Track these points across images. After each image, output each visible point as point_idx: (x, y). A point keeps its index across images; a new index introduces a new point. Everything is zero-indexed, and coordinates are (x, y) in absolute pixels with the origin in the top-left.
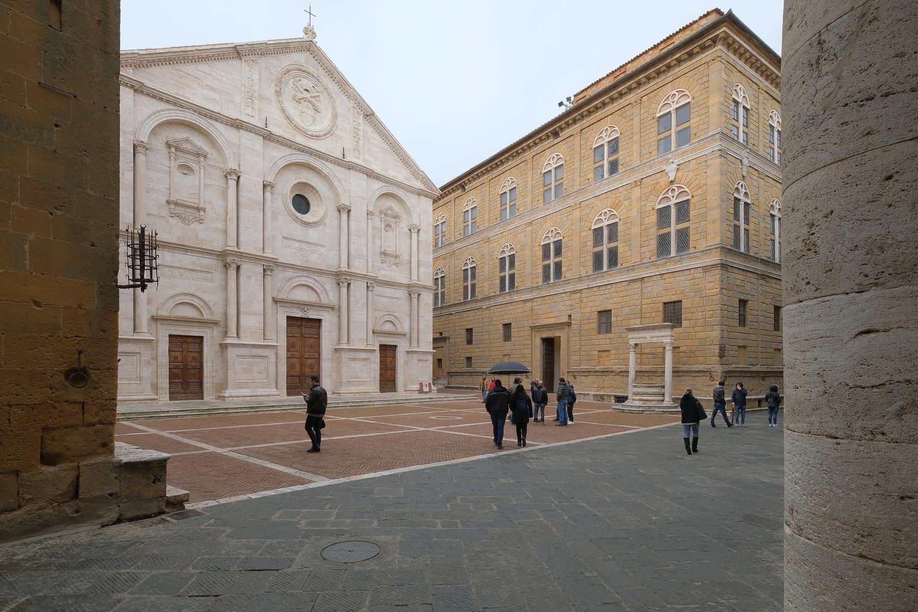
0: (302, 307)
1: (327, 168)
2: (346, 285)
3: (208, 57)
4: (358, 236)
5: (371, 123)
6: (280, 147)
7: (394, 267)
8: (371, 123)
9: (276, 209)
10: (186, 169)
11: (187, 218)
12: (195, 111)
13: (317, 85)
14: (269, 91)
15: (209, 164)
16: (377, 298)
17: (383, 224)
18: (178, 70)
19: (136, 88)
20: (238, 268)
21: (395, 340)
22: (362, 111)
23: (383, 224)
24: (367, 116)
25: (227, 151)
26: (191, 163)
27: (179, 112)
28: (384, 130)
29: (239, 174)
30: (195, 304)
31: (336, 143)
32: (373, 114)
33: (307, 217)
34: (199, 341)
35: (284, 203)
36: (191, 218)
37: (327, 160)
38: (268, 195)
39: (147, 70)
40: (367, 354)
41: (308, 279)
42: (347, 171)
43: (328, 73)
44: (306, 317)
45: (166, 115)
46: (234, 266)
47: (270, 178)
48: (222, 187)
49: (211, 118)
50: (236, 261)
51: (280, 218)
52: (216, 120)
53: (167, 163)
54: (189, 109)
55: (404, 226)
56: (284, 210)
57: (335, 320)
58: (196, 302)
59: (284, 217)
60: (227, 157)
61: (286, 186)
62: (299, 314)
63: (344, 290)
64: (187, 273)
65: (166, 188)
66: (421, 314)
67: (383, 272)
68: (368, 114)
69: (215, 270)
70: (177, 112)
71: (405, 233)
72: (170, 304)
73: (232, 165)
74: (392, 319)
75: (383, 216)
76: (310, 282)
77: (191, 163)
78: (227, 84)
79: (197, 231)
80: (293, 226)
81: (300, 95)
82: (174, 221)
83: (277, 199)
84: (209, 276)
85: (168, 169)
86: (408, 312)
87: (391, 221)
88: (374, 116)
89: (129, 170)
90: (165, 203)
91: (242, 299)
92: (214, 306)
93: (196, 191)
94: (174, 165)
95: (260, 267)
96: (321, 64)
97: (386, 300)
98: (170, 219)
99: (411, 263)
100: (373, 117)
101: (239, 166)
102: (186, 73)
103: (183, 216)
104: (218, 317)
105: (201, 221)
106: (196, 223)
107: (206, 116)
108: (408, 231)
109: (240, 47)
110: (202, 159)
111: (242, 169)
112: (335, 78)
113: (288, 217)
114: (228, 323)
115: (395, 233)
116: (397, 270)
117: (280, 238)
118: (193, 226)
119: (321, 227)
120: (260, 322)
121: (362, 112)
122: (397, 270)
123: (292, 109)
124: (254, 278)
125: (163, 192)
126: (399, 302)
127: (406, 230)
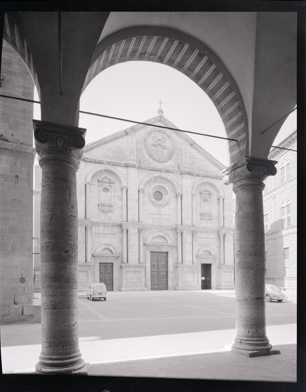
1: (170, 177)
7: (209, 221)
10: (106, 190)
17: (202, 199)
22: (188, 143)
23: (202, 199)
24: (192, 144)
29: (127, 188)
32: (195, 143)
33: (160, 202)
34: (112, 265)
35: (150, 197)
38: (141, 195)
47: (141, 187)
58: (110, 248)
61: (150, 189)
63: (179, 237)
64: (106, 235)
73: (124, 184)
74: (208, 249)
84: (116, 236)
86: (218, 245)
87: (207, 197)
94: (101, 189)
99: (219, 218)
101: (127, 184)
105: (111, 211)
108: (217, 201)
111: (129, 185)
118: (109, 214)
119: (167, 206)
126: (212, 240)
127: (216, 200)
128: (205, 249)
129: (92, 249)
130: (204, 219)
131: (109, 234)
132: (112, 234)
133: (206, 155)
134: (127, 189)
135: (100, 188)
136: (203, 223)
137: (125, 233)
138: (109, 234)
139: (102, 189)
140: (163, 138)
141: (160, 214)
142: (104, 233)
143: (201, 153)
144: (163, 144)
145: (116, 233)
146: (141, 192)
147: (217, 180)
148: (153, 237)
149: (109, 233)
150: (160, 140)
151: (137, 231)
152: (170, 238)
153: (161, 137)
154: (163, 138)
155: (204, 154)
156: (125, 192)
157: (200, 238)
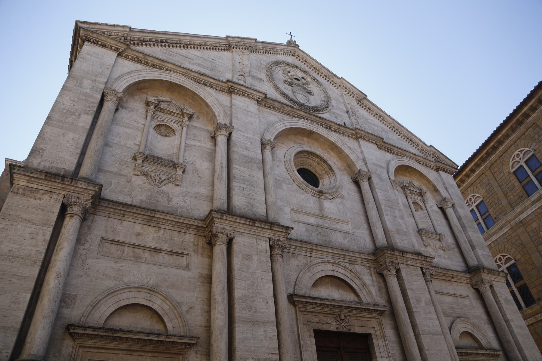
0: (338, 311)
2: (393, 271)
3: (200, 45)
6: (277, 114)
7: (441, 252)
8: (364, 107)
9: (279, 177)
11: (157, 178)
14: (263, 76)
15: (194, 126)
19: (121, 51)
20: (230, 243)
25: (217, 110)
26: (172, 124)
28: (379, 111)
30: (155, 307)
36: (164, 178)
38: (268, 154)
41: (336, 268)
43: (315, 70)
44: (345, 330)
45: (149, 75)
46: (223, 239)
48: (208, 149)
50: (226, 231)
51: (285, 186)
52: (205, 84)
53: (142, 121)
55: (432, 203)
56: (289, 177)
57: (390, 333)
58: (157, 304)
60: (216, 115)
62: (332, 326)
64: (147, 254)
65: (135, 144)
68: (361, 98)
69: (194, 251)
70: (161, 73)
71: (437, 212)
76: (340, 273)
79: (171, 196)
80: (303, 196)
82: (139, 181)
83: (278, 166)
84: (183, 261)
85: (142, 126)
87: (418, 199)
89: (88, 114)
90: (130, 160)
91: (238, 293)
92: (188, 312)
93: (175, 151)
95: (264, 242)
97: (449, 299)
98: (134, 178)
103: (153, 175)
104: (198, 329)
106: (170, 185)
109: (231, 39)
110: (186, 119)
113: (296, 186)
114: (213, 342)
115: (425, 211)
116: (446, 257)
117: (287, 210)
118: (164, 188)
120: (270, 338)
124: (255, 258)
125: (130, 148)
126: (467, 302)
131: (157, 250)
132: (171, 253)
134: (230, 134)
135: (149, 118)
137: (220, 249)
139: (154, 124)
140: (303, 78)
141: (323, 217)
142: (139, 243)
145: (187, 252)
146: (268, 147)
149: (157, 246)
151: (265, 246)
152: (364, 285)
154: (303, 78)
156: (222, 139)
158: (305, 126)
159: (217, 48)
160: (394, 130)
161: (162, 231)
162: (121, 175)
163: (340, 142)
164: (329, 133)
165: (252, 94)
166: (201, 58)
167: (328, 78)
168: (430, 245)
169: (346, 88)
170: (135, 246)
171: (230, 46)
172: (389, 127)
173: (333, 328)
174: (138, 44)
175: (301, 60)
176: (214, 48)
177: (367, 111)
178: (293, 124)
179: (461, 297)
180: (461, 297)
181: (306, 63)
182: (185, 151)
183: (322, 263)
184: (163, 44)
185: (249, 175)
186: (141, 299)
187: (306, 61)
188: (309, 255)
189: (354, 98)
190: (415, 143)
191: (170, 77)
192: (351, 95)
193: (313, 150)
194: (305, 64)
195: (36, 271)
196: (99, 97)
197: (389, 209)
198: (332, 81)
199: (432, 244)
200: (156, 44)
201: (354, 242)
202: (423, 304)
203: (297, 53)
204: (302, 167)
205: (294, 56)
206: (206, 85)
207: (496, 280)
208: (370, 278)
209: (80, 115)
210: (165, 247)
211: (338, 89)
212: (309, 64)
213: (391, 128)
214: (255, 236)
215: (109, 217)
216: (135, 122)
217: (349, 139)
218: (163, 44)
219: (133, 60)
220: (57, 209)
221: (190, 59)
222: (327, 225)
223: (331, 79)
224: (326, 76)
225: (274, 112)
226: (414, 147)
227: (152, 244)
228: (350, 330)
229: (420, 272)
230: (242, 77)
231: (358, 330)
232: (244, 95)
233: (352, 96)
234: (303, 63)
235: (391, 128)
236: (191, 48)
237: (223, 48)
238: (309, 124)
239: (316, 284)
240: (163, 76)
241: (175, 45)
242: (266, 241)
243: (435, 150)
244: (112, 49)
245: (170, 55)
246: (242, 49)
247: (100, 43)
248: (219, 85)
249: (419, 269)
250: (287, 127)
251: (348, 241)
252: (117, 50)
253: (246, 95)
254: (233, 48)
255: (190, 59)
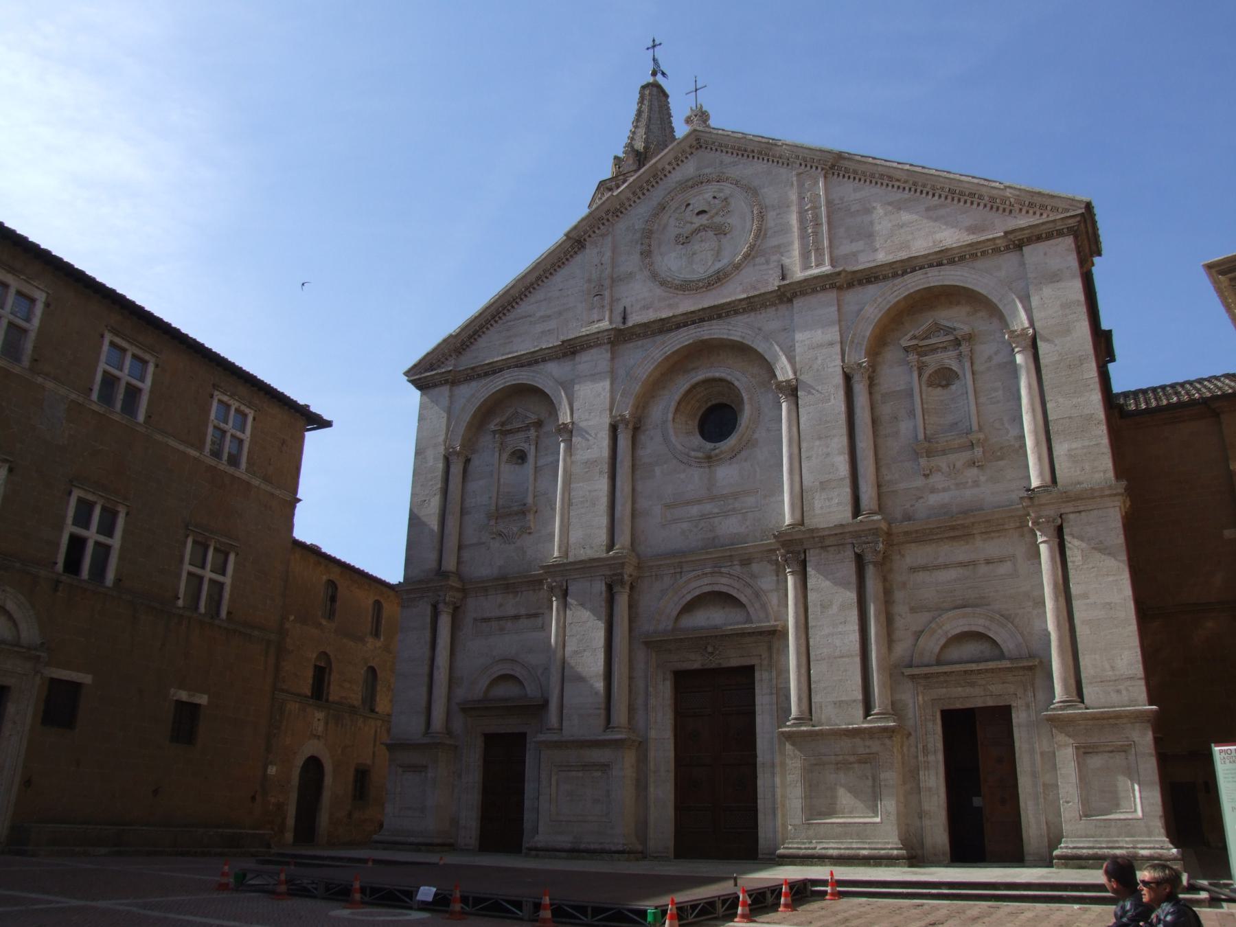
4: (820, 438)
5: (847, 175)
12: (517, 366)
13: (721, 191)
16: (921, 577)
18: (507, 322)
21: (996, 688)
22: (817, 168)
23: (915, 374)
26: (522, 444)
27: (497, 380)
31: (765, 267)
32: (840, 156)
37: (736, 312)
39: (473, 347)
40: (868, 743)
42: (783, 308)
43: (740, 153)
44: (713, 666)
49: (536, 362)
51: (658, 470)
54: (509, 368)
58: (518, 672)
59: (665, 466)
62: (695, 662)
66: (1074, 589)
67: (933, 499)
72: (484, 683)
74: (978, 624)
75: (913, 357)
77: (522, 444)
78: (568, 295)
80: (683, 476)
81: (689, 228)
83: (652, 438)
87: (948, 359)
88: (845, 159)
96: (724, 150)
100: (842, 162)
102: (516, 319)
103: (505, 531)
107: (530, 364)
112: (753, 151)
121: (819, 169)
122: (983, 479)
123: (672, 262)
128: (956, 624)
129: (452, 682)
130: (939, 470)
131: (516, 617)
132: (529, 616)
133: (906, 182)
136: (933, 491)
138: (516, 617)
139: (505, 456)
143: (885, 182)
144: (718, 219)
147: (980, 264)
148: (684, 601)
150: (703, 212)
153: (708, 196)
154: (715, 197)
155: (898, 180)
157: (925, 568)
158: (689, 339)
159: (564, 260)
160: (919, 191)
161: (520, 594)
162: (484, 543)
163: (750, 333)
164: (730, 328)
165: (598, 338)
166: (545, 300)
167: (766, 154)
168: (939, 470)
169: (797, 157)
170: (499, 619)
171: (579, 242)
172: (907, 189)
173: (696, 666)
174: (471, 343)
175: (714, 148)
176: (560, 264)
177: (854, 178)
178: (667, 348)
179: (988, 562)
180: (988, 562)
181: (722, 148)
182: (535, 480)
183: (695, 577)
184: (497, 319)
185: (590, 491)
186: (506, 669)
187: (720, 145)
188: (679, 570)
189: (819, 169)
190: (972, 195)
191: (503, 381)
192: (811, 167)
193: (710, 375)
194: (722, 151)
195: (426, 669)
196: (440, 465)
197: (817, 443)
198: (773, 156)
199: (944, 466)
200: (489, 326)
201: (756, 524)
202: (835, 609)
203: (702, 140)
204: (709, 404)
205: (701, 147)
206: (546, 361)
207: (1081, 508)
208: (775, 578)
209: (429, 500)
210: (523, 611)
211: (790, 167)
212: (727, 146)
213: (913, 189)
214: (590, 578)
215: (477, 596)
216: (487, 465)
217: (777, 310)
218: (497, 319)
219: (466, 380)
220: (429, 610)
221: (530, 316)
222: (716, 510)
223: (770, 154)
224: (760, 153)
225: (640, 343)
226: (975, 205)
227: (512, 612)
228: (720, 664)
229: (849, 554)
230: (597, 297)
231: (734, 662)
232: (591, 346)
233: (814, 168)
234: (719, 152)
235: (913, 189)
236: (530, 292)
237: (572, 253)
238: (694, 331)
239: (690, 607)
240: (498, 383)
241: (509, 308)
242: (601, 580)
243: (1018, 193)
244: (442, 384)
245: (508, 330)
246: (599, 228)
247: (431, 385)
248: (557, 351)
249: (849, 547)
250: (656, 363)
251: (747, 527)
252: (446, 382)
253: (592, 344)
254: (585, 240)
255: (530, 316)
